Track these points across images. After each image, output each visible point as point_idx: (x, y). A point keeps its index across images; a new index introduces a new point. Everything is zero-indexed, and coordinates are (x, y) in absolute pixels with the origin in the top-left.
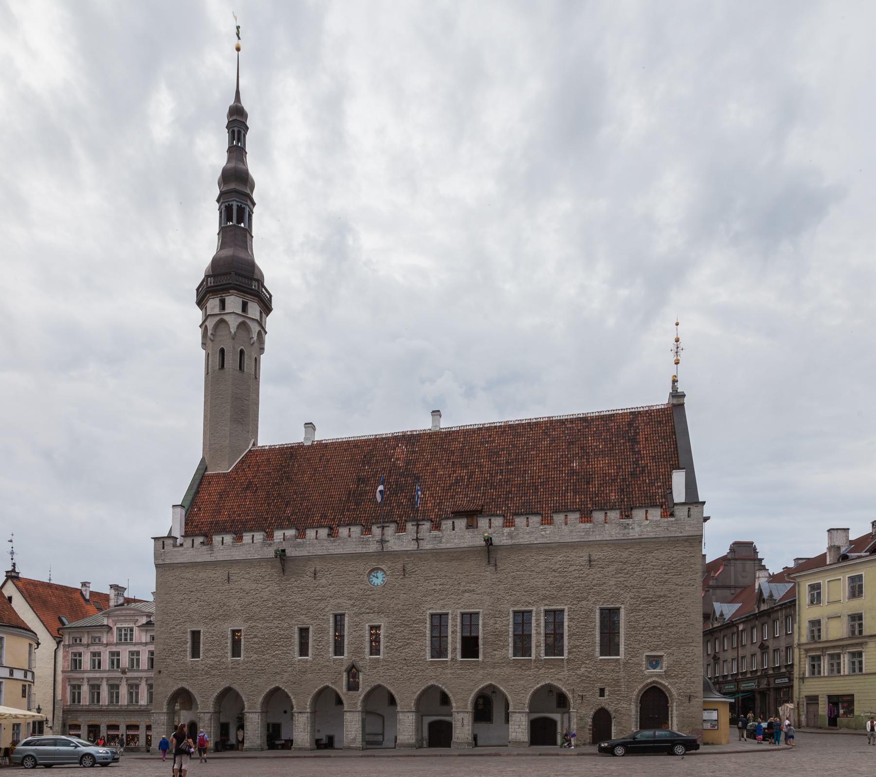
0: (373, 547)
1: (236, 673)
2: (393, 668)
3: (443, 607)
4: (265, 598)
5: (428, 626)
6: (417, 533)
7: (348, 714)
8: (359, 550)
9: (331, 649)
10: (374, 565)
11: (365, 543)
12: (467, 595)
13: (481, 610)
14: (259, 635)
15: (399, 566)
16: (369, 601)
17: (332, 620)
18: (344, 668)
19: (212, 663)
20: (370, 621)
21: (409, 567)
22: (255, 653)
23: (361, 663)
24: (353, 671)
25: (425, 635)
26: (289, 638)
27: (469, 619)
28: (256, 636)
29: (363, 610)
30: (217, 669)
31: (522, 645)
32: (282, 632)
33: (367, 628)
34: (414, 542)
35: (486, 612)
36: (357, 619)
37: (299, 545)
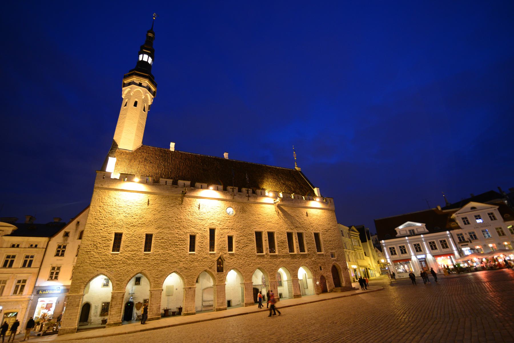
1: (147, 262)
2: (241, 259)
3: (260, 228)
4: (171, 216)
6: (248, 193)
12: (269, 223)
14: (165, 237)
18: (216, 259)
19: (129, 255)
22: (162, 249)
25: (253, 242)
27: (271, 235)
28: (163, 238)
29: (225, 227)
30: (132, 259)
31: (291, 249)
32: (180, 237)
34: (247, 198)
36: (222, 231)
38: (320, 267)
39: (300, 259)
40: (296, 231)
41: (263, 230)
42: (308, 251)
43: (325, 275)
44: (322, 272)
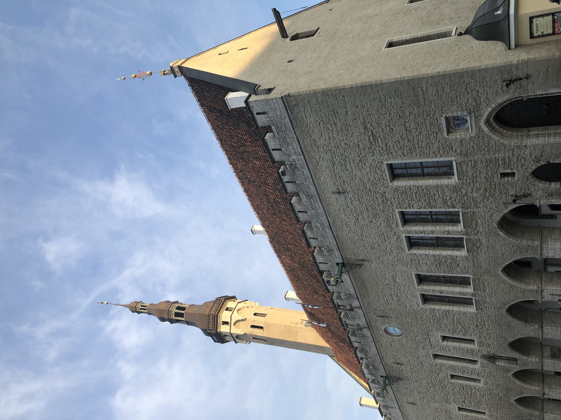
0: (366, 332)
5: (437, 307)
7: (545, 368)
8: (370, 339)
9: (470, 366)
10: (382, 332)
11: (363, 336)
13: (413, 274)
15: (381, 319)
16: (418, 339)
17: (439, 361)
20: (438, 341)
21: (378, 314)
23: (485, 353)
24: (492, 358)
26: (462, 386)
33: (445, 343)
35: (414, 269)
36: (437, 349)
37: (375, 368)
38: (504, 175)
39: (481, 230)
40: (402, 229)
41: (418, 293)
42: (454, 207)
43: (534, 168)
44: (522, 174)
